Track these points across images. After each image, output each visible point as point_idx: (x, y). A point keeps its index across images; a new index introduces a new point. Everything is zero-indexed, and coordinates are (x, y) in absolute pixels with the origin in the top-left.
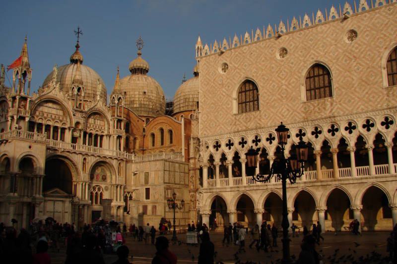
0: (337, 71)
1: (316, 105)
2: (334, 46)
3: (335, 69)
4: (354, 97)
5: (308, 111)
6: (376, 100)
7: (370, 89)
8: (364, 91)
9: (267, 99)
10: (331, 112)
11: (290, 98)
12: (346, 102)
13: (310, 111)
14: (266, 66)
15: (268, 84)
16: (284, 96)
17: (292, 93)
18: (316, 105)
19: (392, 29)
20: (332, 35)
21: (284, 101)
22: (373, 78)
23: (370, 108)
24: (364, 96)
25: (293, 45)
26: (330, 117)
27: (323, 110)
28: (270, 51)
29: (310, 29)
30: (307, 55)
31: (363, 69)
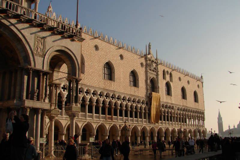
1: (108, 82)
6: (127, 90)
9: (88, 69)
10: (113, 88)
11: (98, 74)
14: (89, 50)
15: (89, 61)
16: (96, 72)
17: (99, 72)
18: (108, 82)
21: (96, 74)
23: (125, 93)
25: (101, 47)
26: (113, 91)
28: (91, 43)
30: (106, 56)
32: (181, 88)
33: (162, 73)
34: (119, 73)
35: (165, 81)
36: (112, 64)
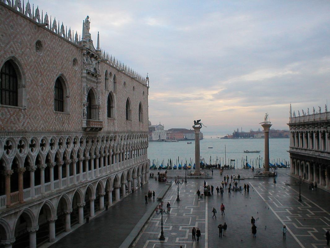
0: (29, 80)
1: (12, 112)
2: (29, 50)
3: (28, 77)
4: (38, 113)
5: (5, 118)
7: (47, 110)
8: (44, 110)
10: (23, 125)
12: (34, 117)
13: (6, 120)
19: (60, 60)
20: (28, 35)
22: (49, 99)
24: (44, 115)
27: (18, 122)
29: (12, 13)
30: (8, 44)
31: (45, 87)
32: (126, 102)
33: (105, 77)
34: (35, 86)
35: (107, 91)
36: (20, 65)
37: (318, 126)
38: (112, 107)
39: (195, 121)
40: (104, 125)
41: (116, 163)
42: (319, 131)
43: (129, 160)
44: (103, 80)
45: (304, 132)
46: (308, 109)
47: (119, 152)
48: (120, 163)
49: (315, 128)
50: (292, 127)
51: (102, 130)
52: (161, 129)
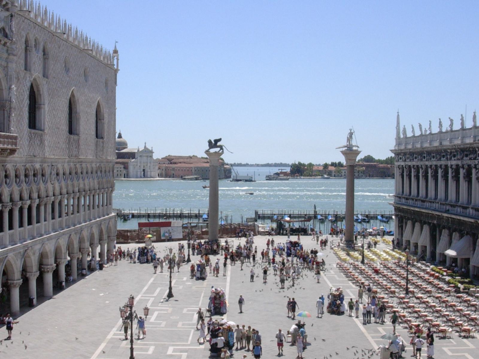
32: (69, 98)
33: (24, 46)
35: (28, 75)
37: (447, 155)
38: (40, 108)
39: (210, 142)
40: (21, 142)
41: (45, 220)
42: (449, 165)
43: (72, 216)
44: (19, 53)
45: (422, 168)
46: (430, 121)
47: (53, 200)
48: (54, 220)
49: (442, 159)
50: (400, 156)
51: (16, 153)
52: (147, 156)
